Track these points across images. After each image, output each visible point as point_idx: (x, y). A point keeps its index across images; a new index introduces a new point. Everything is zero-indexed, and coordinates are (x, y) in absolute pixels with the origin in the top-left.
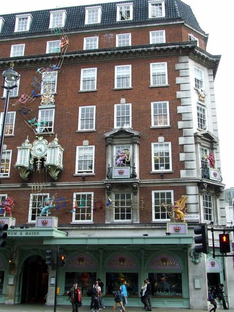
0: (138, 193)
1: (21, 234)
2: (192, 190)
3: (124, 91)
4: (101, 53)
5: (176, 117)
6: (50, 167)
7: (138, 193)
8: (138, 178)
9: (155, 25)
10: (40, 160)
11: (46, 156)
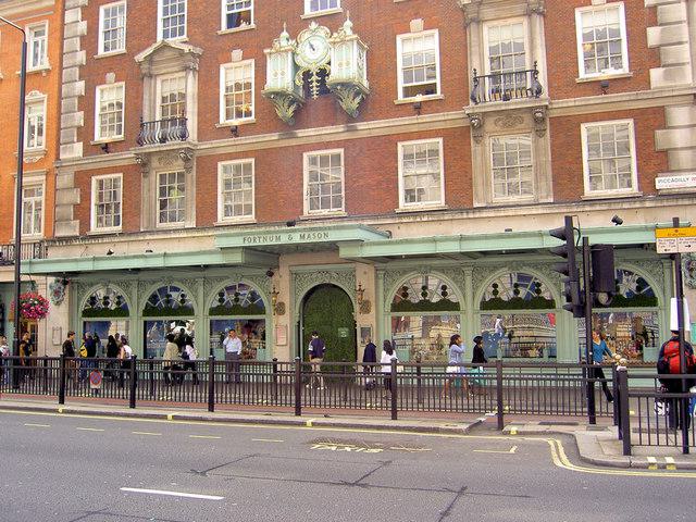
0: (548, 131)
8: (545, 94)
10: (317, 74)
11: (329, 63)
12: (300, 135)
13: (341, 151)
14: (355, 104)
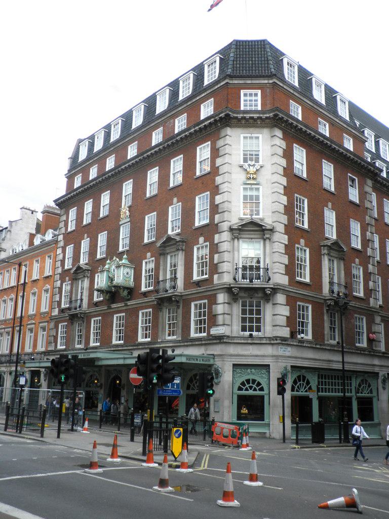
0: (181, 306)
2: (221, 297)
4: (155, 150)
5: (214, 209)
7: (181, 306)
9: (203, 95)
14: (125, 293)
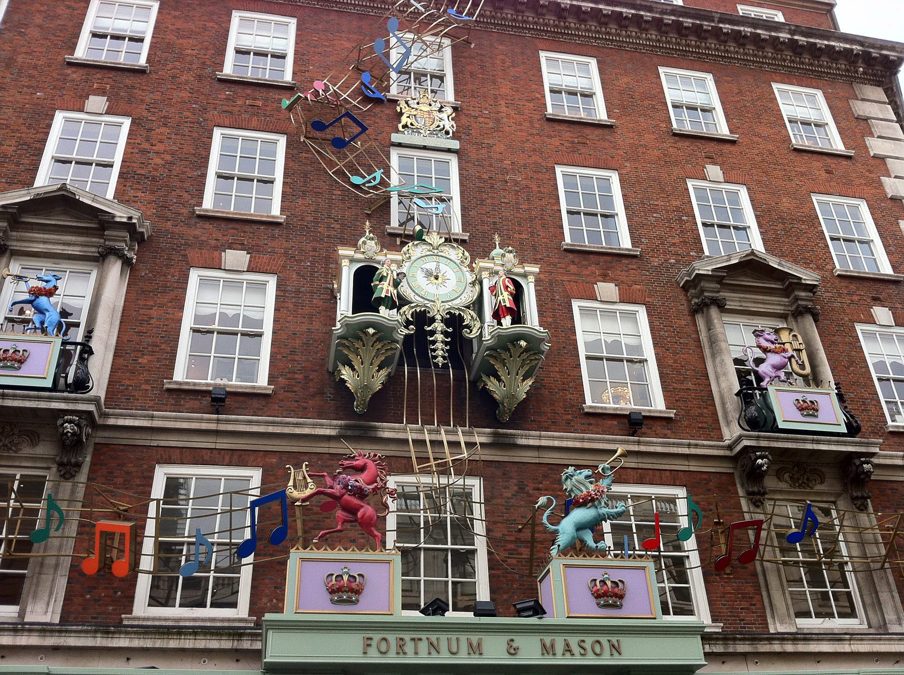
1: (513, 651)
3: (712, 144)
6: (523, 343)
12: (387, 435)
13: (475, 485)
